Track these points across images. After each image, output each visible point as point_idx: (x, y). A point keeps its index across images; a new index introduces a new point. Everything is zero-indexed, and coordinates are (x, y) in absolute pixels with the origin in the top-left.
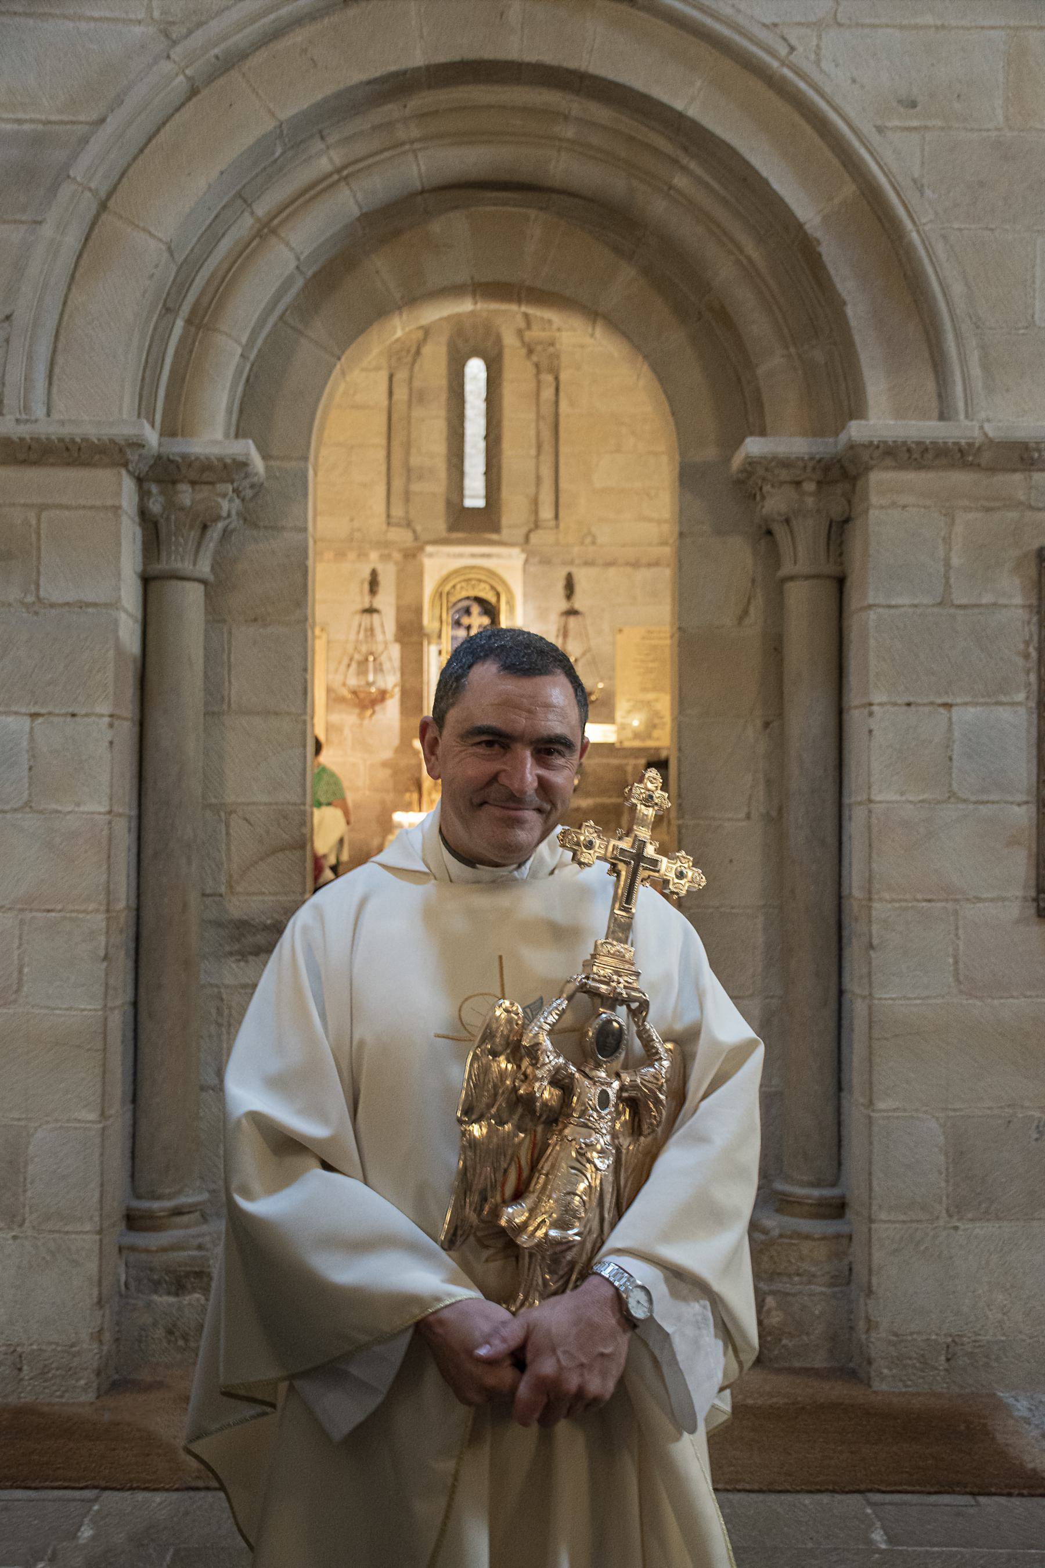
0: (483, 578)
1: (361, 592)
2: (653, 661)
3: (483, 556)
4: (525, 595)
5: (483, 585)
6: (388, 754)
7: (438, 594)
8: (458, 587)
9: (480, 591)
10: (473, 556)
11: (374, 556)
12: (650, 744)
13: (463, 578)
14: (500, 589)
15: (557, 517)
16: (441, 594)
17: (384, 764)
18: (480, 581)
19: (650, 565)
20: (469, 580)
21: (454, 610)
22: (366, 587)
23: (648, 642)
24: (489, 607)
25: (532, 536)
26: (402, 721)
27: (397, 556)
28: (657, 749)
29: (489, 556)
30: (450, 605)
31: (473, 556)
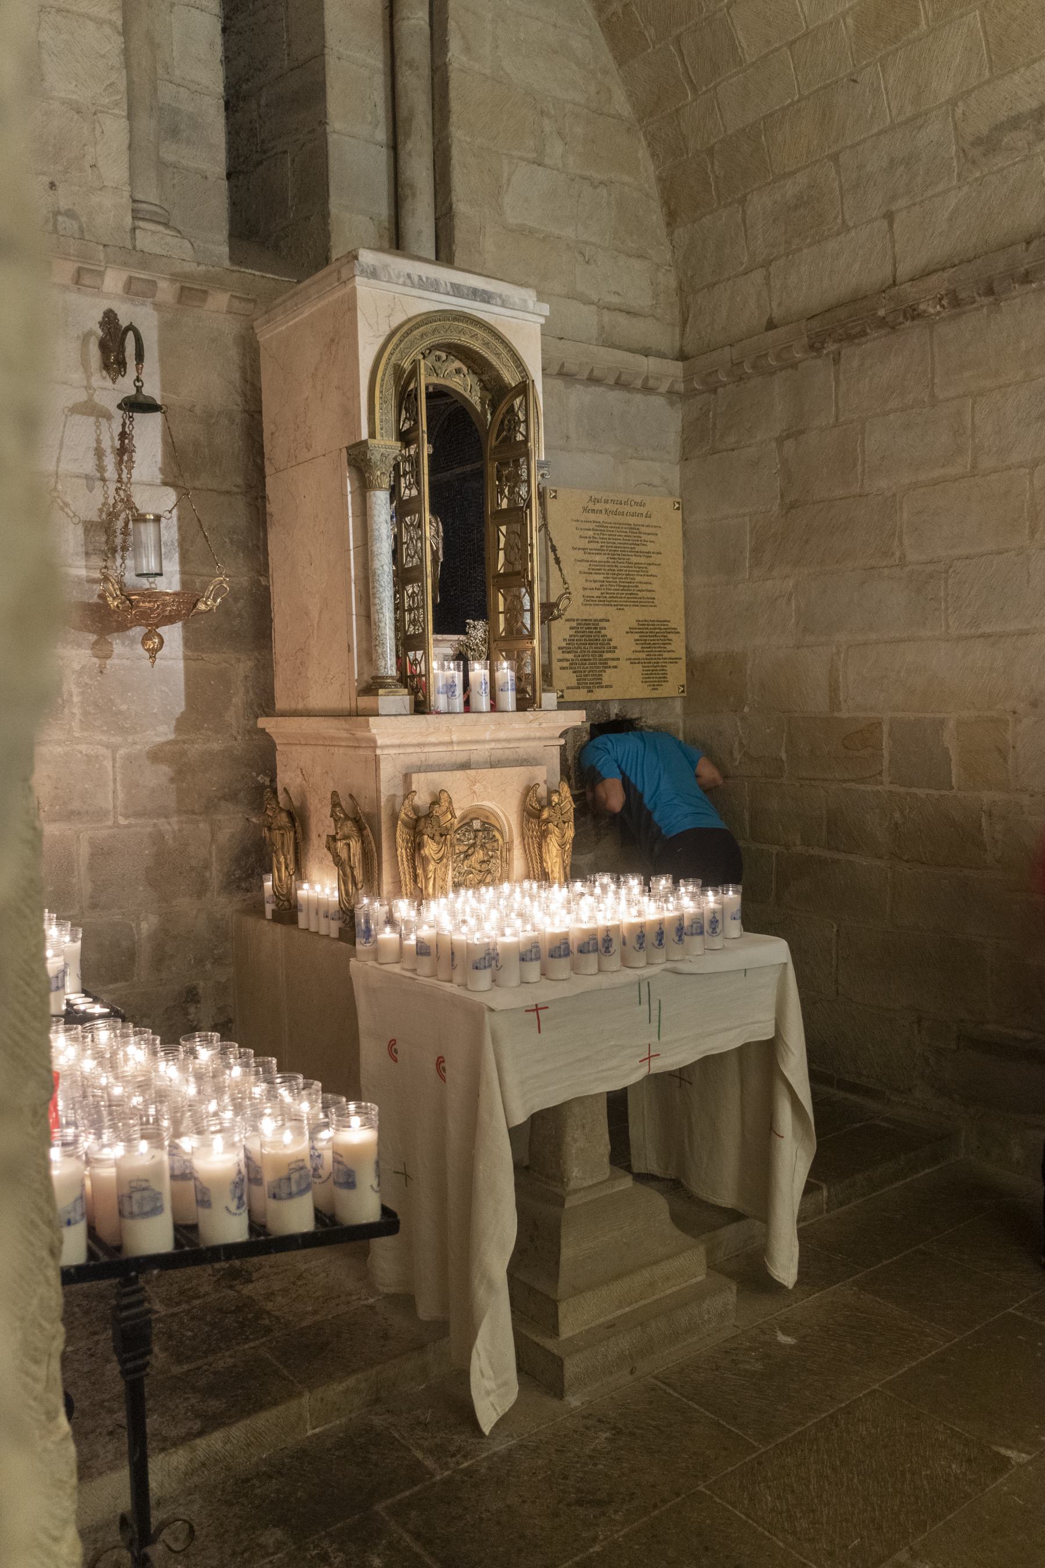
1: (85, 364)
2: (599, 551)
3: (476, 294)
6: (163, 733)
10: (457, 290)
11: (113, 280)
12: (600, 694)
17: (156, 755)
19: (593, 380)
22: (95, 353)
23: (592, 517)
26: (186, 658)
27: (166, 290)
28: (605, 702)
29: (485, 297)
31: (457, 290)
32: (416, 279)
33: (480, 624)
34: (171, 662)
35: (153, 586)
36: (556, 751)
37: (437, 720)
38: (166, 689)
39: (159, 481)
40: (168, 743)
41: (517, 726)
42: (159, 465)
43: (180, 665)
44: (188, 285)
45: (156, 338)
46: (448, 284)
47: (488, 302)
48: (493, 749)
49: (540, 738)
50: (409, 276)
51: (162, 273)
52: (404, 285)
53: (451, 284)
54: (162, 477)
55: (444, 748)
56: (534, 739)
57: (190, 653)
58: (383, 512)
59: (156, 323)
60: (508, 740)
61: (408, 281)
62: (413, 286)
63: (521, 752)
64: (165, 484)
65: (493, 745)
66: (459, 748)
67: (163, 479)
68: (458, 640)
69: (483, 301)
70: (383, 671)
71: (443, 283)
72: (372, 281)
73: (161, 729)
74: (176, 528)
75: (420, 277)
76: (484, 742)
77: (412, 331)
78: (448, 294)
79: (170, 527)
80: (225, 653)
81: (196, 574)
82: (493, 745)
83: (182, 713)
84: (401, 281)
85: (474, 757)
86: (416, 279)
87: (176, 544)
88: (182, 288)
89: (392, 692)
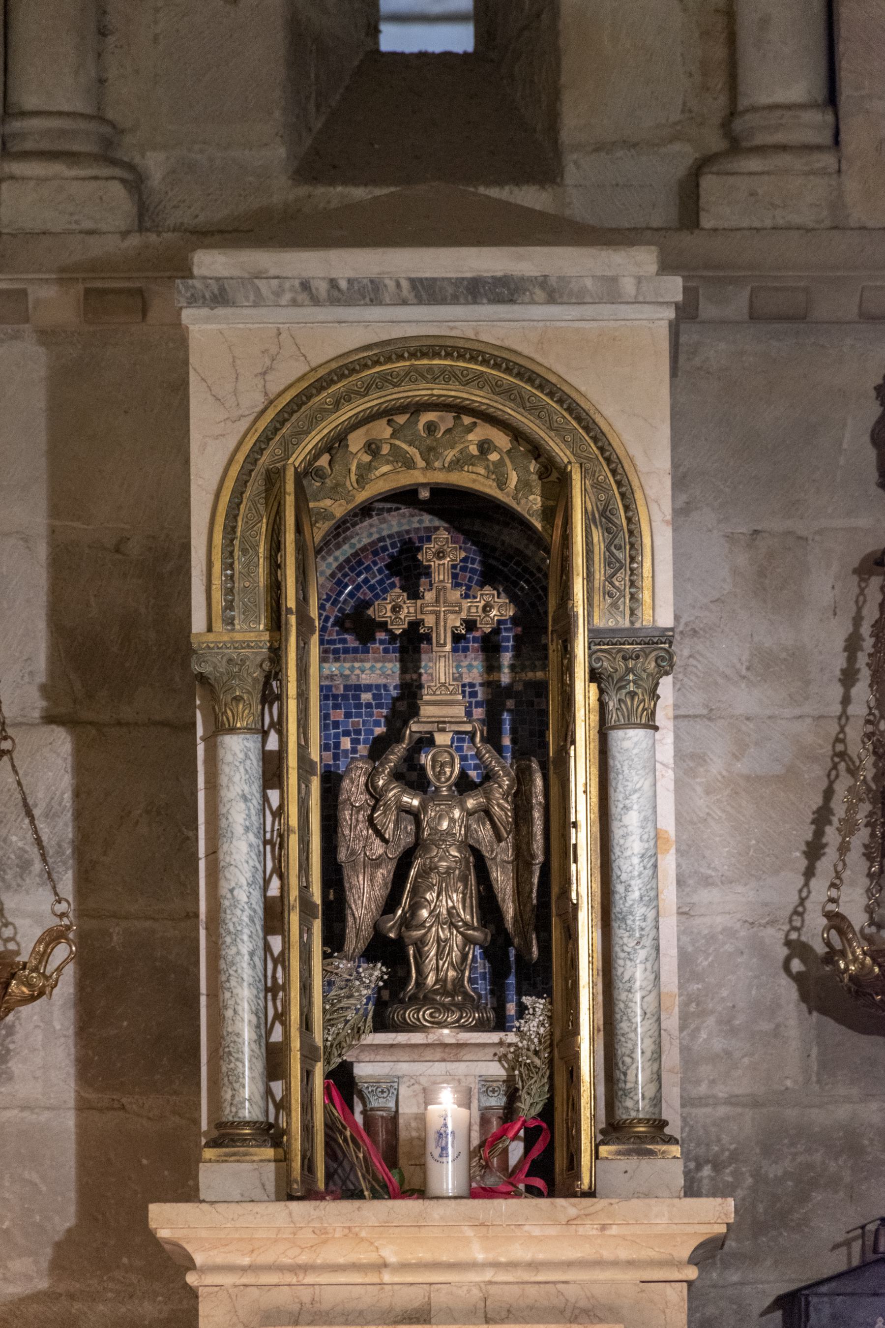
0: (478, 397)
4: (680, 482)
5: (484, 431)
7: (255, 486)
8: (356, 441)
9: (456, 465)
13: (371, 402)
14: (561, 453)
15: (832, 99)
16: (273, 478)
18: (459, 409)
20: (417, 408)
21: (330, 564)
24: (511, 538)
25: (709, 183)
26: (83, 1107)
30: (321, 530)
32: (322, 288)
33: (537, 1005)
34: (45, 1116)
35: (12, 946)
36: (677, 1296)
37: (315, 1214)
38: (35, 1177)
39: (37, 714)
40: (36, 1297)
41: (536, 1232)
42: (41, 677)
43: (69, 1121)
44: (99, 284)
45: (43, 404)
46: (405, 284)
47: (512, 301)
48: (490, 1283)
49: (630, 1264)
50: (305, 286)
51: (39, 271)
52: (294, 303)
53: (413, 281)
54: (44, 704)
55: (357, 1278)
56: (615, 1264)
57: (92, 1096)
58: (237, 778)
59: (43, 373)
60: (533, 1266)
61: (303, 297)
62: (316, 301)
63: (571, 1292)
64: (50, 719)
65: (488, 1275)
66: (397, 1279)
67: (46, 710)
68: (501, 1043)
69: (498, 300)
70: (227, 1112)
71: (391, 284)
72: (221, 311)
73: (19, 1265)
74: (68, 816)
75: (333, 283)
76: (472, 1266)
77: (309, 398)
78: (404, 303)
79: (56, 815)
80: (175, 1093)
81: (115, 916)
82: (488, 1275)
83: (69, 1231)
84: (287, 297)
85: (440, 1298)
86: (322, 288)
87: (69, 851)
88: (88, 292)
89: (234, 1154)
